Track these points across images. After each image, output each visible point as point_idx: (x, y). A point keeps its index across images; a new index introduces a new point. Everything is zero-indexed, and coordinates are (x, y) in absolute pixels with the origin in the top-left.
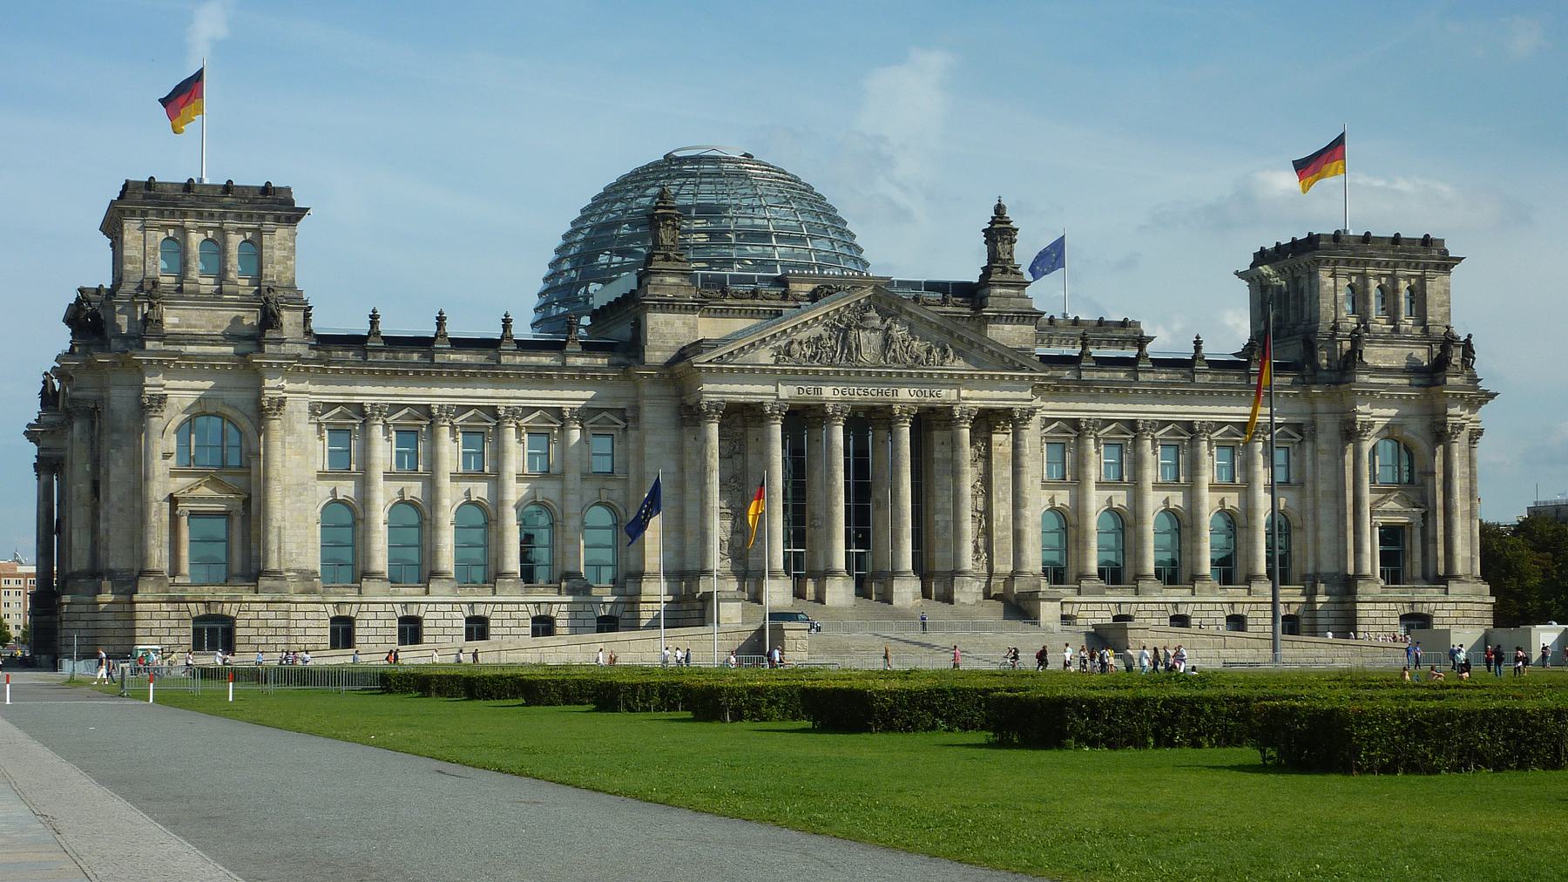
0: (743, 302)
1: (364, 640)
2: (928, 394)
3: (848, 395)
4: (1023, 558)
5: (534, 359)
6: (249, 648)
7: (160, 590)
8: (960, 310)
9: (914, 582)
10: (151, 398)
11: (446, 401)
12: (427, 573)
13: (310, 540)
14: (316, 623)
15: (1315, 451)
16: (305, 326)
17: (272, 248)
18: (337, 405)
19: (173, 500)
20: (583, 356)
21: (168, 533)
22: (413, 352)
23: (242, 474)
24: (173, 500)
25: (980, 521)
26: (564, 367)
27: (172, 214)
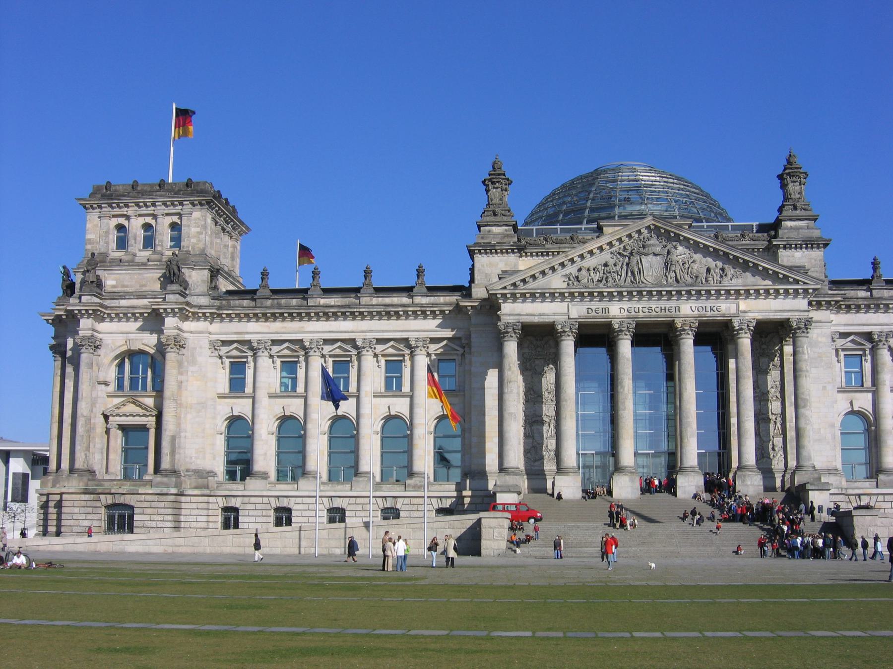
0: (562, 245)
2: (708, 309)
3: (633, 313)
4: (804, 453)
5: (388, 300)
6: (143, 530)
7: (81, 484)
8: (757, 242)
9: (696, 477)
10: (84, 338)
14: (205, 512)
16: (211, 281)
17: (189, 226)
20: (427, 296)
24: (106, 417)
25: (775, 423)
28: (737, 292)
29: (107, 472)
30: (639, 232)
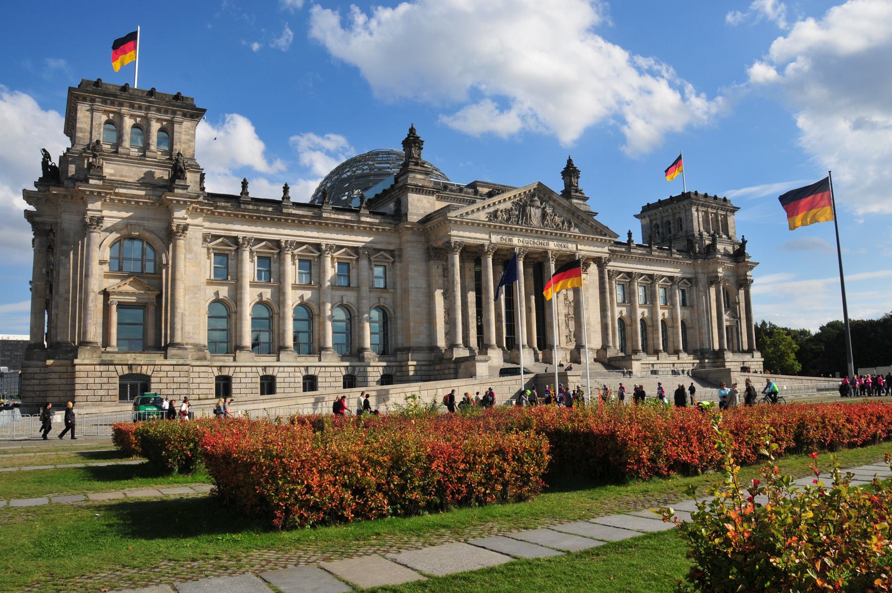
1: (238, 391)
5: (341, 217)
7: (95, 355)
10: (92, 218)
11: (290, 239)
12: (276, 348)
13: (201, 325)
14: (206, 380)
15: (698, 291)
17: (181, 133)
18: (219, 237)
19: (106, 294)
21: (102, 316)
22: (269, 207)
23: (154, 278)
24: (106, 294)
26: (359, 222)
27: (113, 104)
28: (579, 237)
29: (106, 343)
30: (530, 191)
